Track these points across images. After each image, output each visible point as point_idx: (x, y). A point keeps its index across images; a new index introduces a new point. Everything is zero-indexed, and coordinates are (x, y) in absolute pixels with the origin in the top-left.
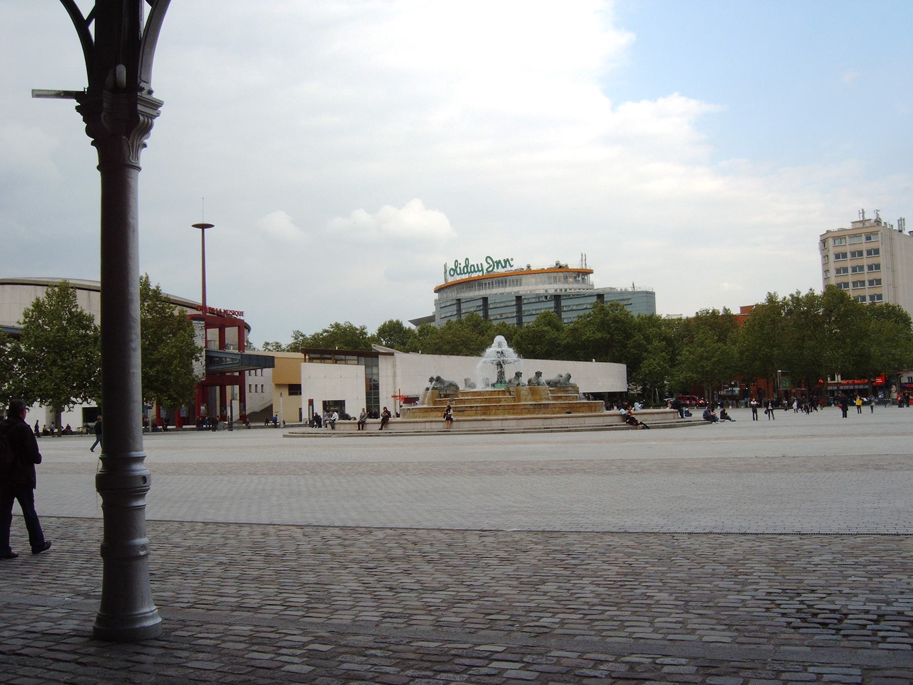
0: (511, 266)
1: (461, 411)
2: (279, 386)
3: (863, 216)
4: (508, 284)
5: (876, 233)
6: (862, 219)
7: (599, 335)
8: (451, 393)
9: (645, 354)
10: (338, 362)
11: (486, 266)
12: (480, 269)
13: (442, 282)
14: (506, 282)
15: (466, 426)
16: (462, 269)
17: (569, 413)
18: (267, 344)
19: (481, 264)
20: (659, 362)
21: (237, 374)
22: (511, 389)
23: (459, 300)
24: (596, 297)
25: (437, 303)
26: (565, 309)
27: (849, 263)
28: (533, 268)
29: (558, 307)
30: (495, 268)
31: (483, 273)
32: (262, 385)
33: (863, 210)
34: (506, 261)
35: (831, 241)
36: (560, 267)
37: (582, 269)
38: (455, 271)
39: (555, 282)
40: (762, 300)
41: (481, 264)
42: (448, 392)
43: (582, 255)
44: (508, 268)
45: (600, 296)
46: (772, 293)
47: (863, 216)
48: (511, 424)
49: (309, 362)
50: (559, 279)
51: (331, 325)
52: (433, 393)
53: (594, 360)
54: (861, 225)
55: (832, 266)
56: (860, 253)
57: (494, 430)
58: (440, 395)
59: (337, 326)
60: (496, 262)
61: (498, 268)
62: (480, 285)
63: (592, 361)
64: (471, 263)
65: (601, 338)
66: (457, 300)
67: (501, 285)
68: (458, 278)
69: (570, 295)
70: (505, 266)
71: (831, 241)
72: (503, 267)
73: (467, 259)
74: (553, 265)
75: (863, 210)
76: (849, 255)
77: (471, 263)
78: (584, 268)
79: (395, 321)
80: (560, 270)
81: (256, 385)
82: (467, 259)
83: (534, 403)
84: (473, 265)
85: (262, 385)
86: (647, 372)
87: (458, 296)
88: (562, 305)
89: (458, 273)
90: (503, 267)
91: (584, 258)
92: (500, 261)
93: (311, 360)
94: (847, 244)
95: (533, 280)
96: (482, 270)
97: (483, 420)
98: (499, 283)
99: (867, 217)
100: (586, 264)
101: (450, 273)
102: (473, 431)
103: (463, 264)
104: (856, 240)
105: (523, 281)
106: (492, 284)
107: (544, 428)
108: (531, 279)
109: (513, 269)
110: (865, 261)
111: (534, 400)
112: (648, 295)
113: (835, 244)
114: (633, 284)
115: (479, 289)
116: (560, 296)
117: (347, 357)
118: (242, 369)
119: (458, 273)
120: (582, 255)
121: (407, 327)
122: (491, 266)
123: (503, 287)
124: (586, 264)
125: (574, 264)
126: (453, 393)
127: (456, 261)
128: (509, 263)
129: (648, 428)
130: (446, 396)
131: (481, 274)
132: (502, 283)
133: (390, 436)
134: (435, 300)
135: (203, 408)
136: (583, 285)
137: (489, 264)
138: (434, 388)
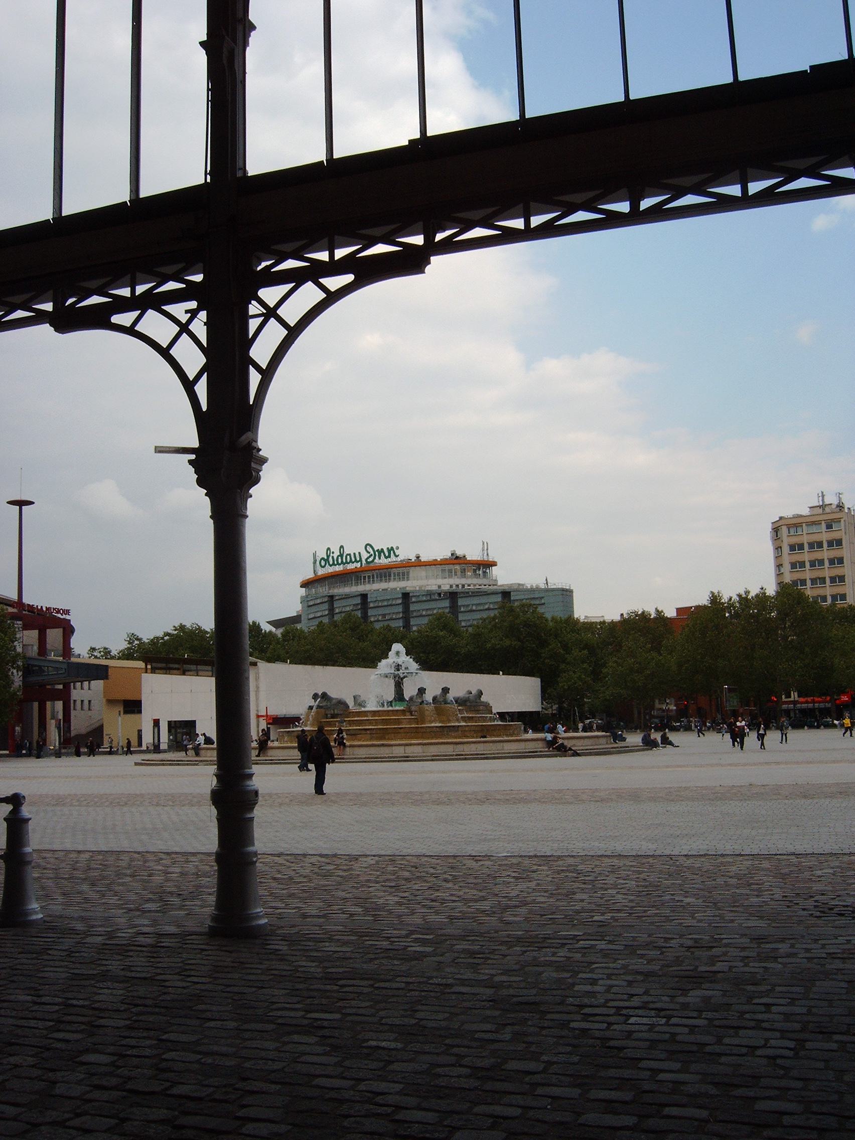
0: (397, 556)
1: (353, 735)
2: (111, 702)
3: (823, 500)
4: (392, 577)
5: (838, 521)
6: (821, 504)
7: (507, 642)
8: (339, 712)
9: (563, 666)
10: (187, 673)
11: (365, 555)
12: (358, 559)
13: (310, 575)
14: (390, 576)
15: (362, 752)
16: (335, 558)
17: (485, 737)
18: (93, 649)
19: (359, 553)
20: (580, 676)
21: (61, 687)
22: (413, 708)
24: (500, 595)
25: (304, 600)
27: (806, 556)
28: (423, 559)
29: (454, 607)
30: (377, 557)
31: (361, 564)
32: (90, 701)
33: (822, 493)
34: (391, 550)
35: (784, 530)
36: (457, 558)
38: (327, 560)
39: (450, 577)
40: (703, 600)
41: (359, 553)
42: (336, 712)
43: (483, 544)
44: (393, 558)
45: (506, 594)
46: (716, 592)
47: (823, 500)
48: (416, 750)
49: (151, 673)
50: (455, 572)
51: (175, 627)
52: (317, 713)
53: (501, 673)
54: (820, 511)
55: (786, 560)
56: (820, 545)
57: (397, 757)
58: (327, 715)
59: (182, 627)
61: (380, 558)
63: (499, 674)
64: (347, 552)
68: (330, 570)
69: (468, 593)
70: (389, 556)
71: (784, 530)
72: (386, 557)
73: (342, 547)
75: (822, 493)
76: (806, 547)
77: (347, 552)
80: (456, 561)
81: (82, 701)
82: (342, 547)
83: (440, 725)
84: (350, 555)
85: (90, 701)
86: (566, 687)
87: (330, 591)
88: (459, 604)
89: (331, 563)
90: (386, 557)
91: (485, 547)
92: (382, 549)
93: (154, 671)
94: (805, 532)
96: (361, 560)
97: (383, 745)
98: (381, 577)
99: (827, 502)
100: (488, 555)
101: (320, 563)
102: (372, 758)
103: (337, 553)
104: (814, 529)
105: (411, 575)
106: (373, 578)
107: (456, 755)
108: (421, 572)
109: (399, 559)
110: (826, 554)
111: (441, 722)
112: (565, 593)
113: (789, 533)
114: (546, 580)
116: (456, 593)
117: (199, 667)
118: (67, 681)
119: (331, 563)
120: (483, 544)
122: (371, 555)
123: (386, 582)
124: (488, 555)
125: (473, 554)
127: (329, 549)
128: (394, 553)
129: (578, 755)
130: (333, 716)
131: (359, 565)
133: (271, 764)
134: (302, 597)
135: (18, 729)
136: (484, 579)
137: (368, 552)
138: (319, 707)
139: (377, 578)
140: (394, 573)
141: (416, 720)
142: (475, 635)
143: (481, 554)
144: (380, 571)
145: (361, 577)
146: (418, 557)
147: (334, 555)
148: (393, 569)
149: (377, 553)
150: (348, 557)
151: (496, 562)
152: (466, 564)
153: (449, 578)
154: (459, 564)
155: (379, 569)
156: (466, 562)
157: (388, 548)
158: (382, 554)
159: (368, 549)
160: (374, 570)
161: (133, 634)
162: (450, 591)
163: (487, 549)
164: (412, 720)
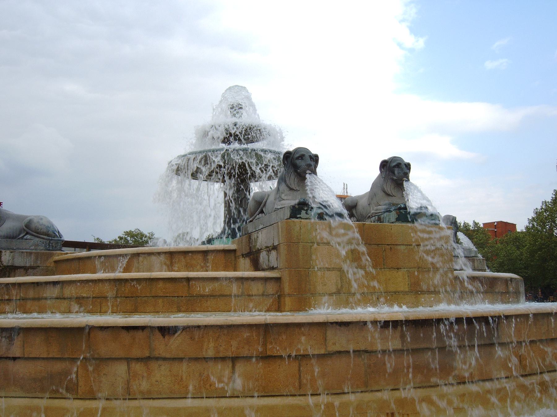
8: (19, 261)
43: (344, 185)
78: (346, 194)
100: (347, 192)
120: (344, 185)
126: (28, 262)
141: (271, 288)
161: (98, 238)
163: (347, 189)
164: (257, 288)
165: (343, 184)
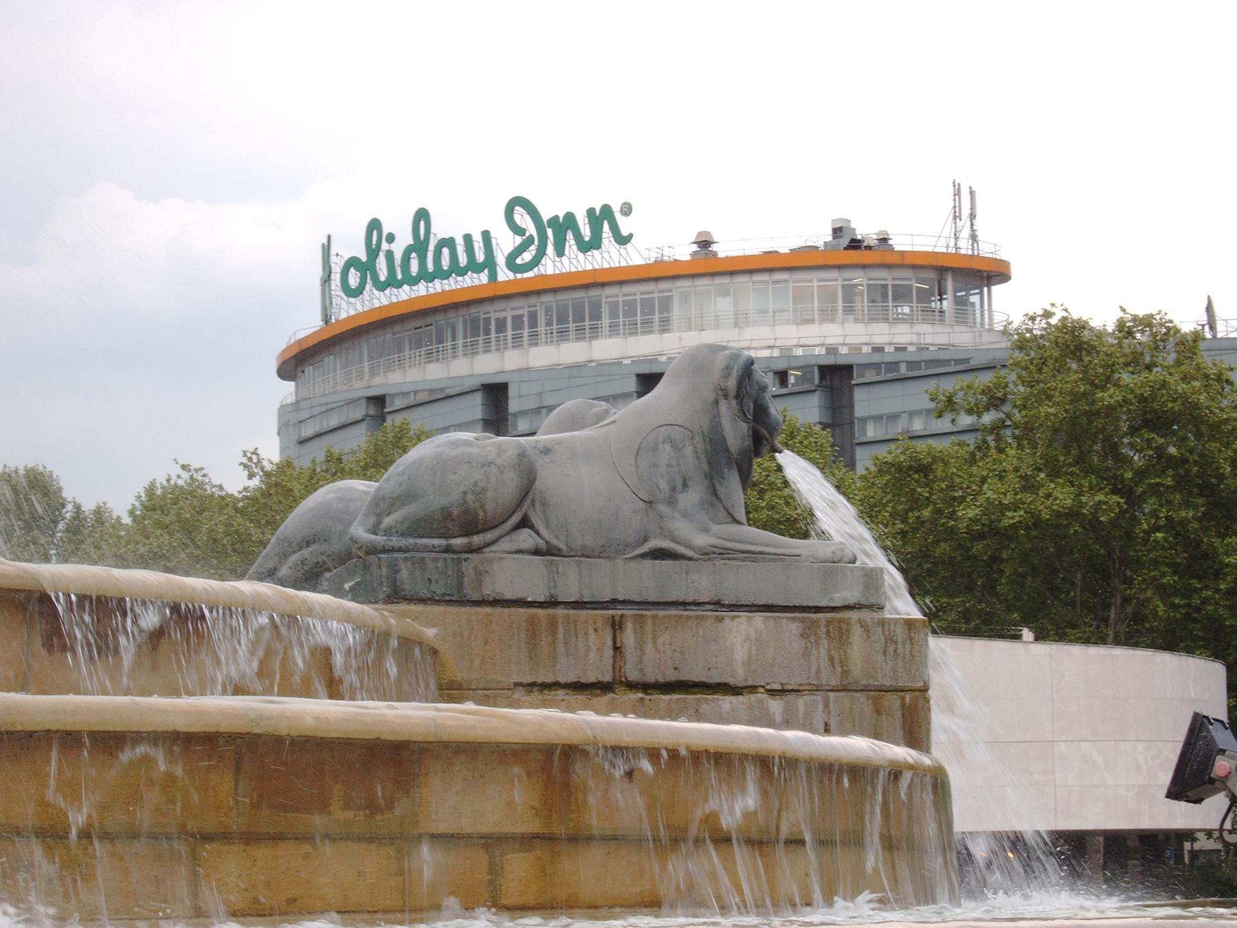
0: (623, 240)
4: (605, 321)
7: (1062, 496)
11: (505, 242)
12: (480, 256)
13: (308, 324)
14: (596, 316)
16: (398, 256)
19: (486, 235)
23: (379, 401)
25: (289, 418)
26: (871, 433)
28: (724, 249)
30: (550, 249)
31: (493, 276)
34: (601, 217)
36: (855, 244)
37: (957, 256)
38: (365, 267)
39: (828, 316)
43: (957, 193)
44: (609, 257)
60: (554, 221)
61: (560, 252)
62: (477, 328)
63: (1017, 637)
64: (440, 230)
65: (1072, 514)
66: (371, 399)
67: (572, 326)
68: (377, 300)
69: (894, 365)
73: (422, 215)
74: (821, 236)
77: (440, 230)
78: (965, 247)
79: (21, 468)
82: (422, 215)
84: (449, 243)
87: (377, 381)
88: (860, 410)
89: (382, 278)
90: (585, 247)
92: (570, 217)
95: (724, 306)
96: (490, 263)
98: (562, 319)
100: (974, 237)
103: (404, 239)
105: (676, 312)
106: (533, 323)
109: (636, 256)
114: (1209, 309)
115: (471, 349)
116: (849, 368)
119: (382, 278)
120: (957, 193)
121: (88, 506)
122: (531, 239)
123: (580, 338)
124: (974, 237)
127: (375, 225)
131: (484, 278)
132: (579, 318)
134: (284, 410)
139: (549, 324)
140: (614, 308)
142: (899, 467)
143: (949, 230)
144: (562, 297)
145: (487, 321)
146: (705, 243)
147: (393, 247)
148: (609, 291)
149: (550, 232)
150: (445, 251)
151: (1006, 264)
152: (889, 267)
153: (822, 321)
154: (864, 267)
155: (554, 291)
156: (889, 259)
157: (591, 212)
158: (570, 235)
159: (517, 218)
160: (538, 293)
162: (823, 362)
163: (972, 216)
165: (950, 191)
